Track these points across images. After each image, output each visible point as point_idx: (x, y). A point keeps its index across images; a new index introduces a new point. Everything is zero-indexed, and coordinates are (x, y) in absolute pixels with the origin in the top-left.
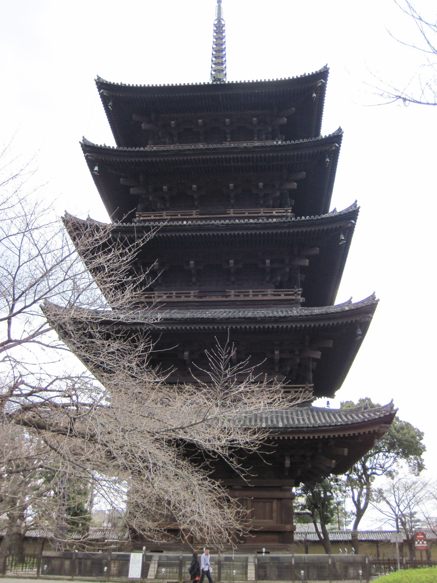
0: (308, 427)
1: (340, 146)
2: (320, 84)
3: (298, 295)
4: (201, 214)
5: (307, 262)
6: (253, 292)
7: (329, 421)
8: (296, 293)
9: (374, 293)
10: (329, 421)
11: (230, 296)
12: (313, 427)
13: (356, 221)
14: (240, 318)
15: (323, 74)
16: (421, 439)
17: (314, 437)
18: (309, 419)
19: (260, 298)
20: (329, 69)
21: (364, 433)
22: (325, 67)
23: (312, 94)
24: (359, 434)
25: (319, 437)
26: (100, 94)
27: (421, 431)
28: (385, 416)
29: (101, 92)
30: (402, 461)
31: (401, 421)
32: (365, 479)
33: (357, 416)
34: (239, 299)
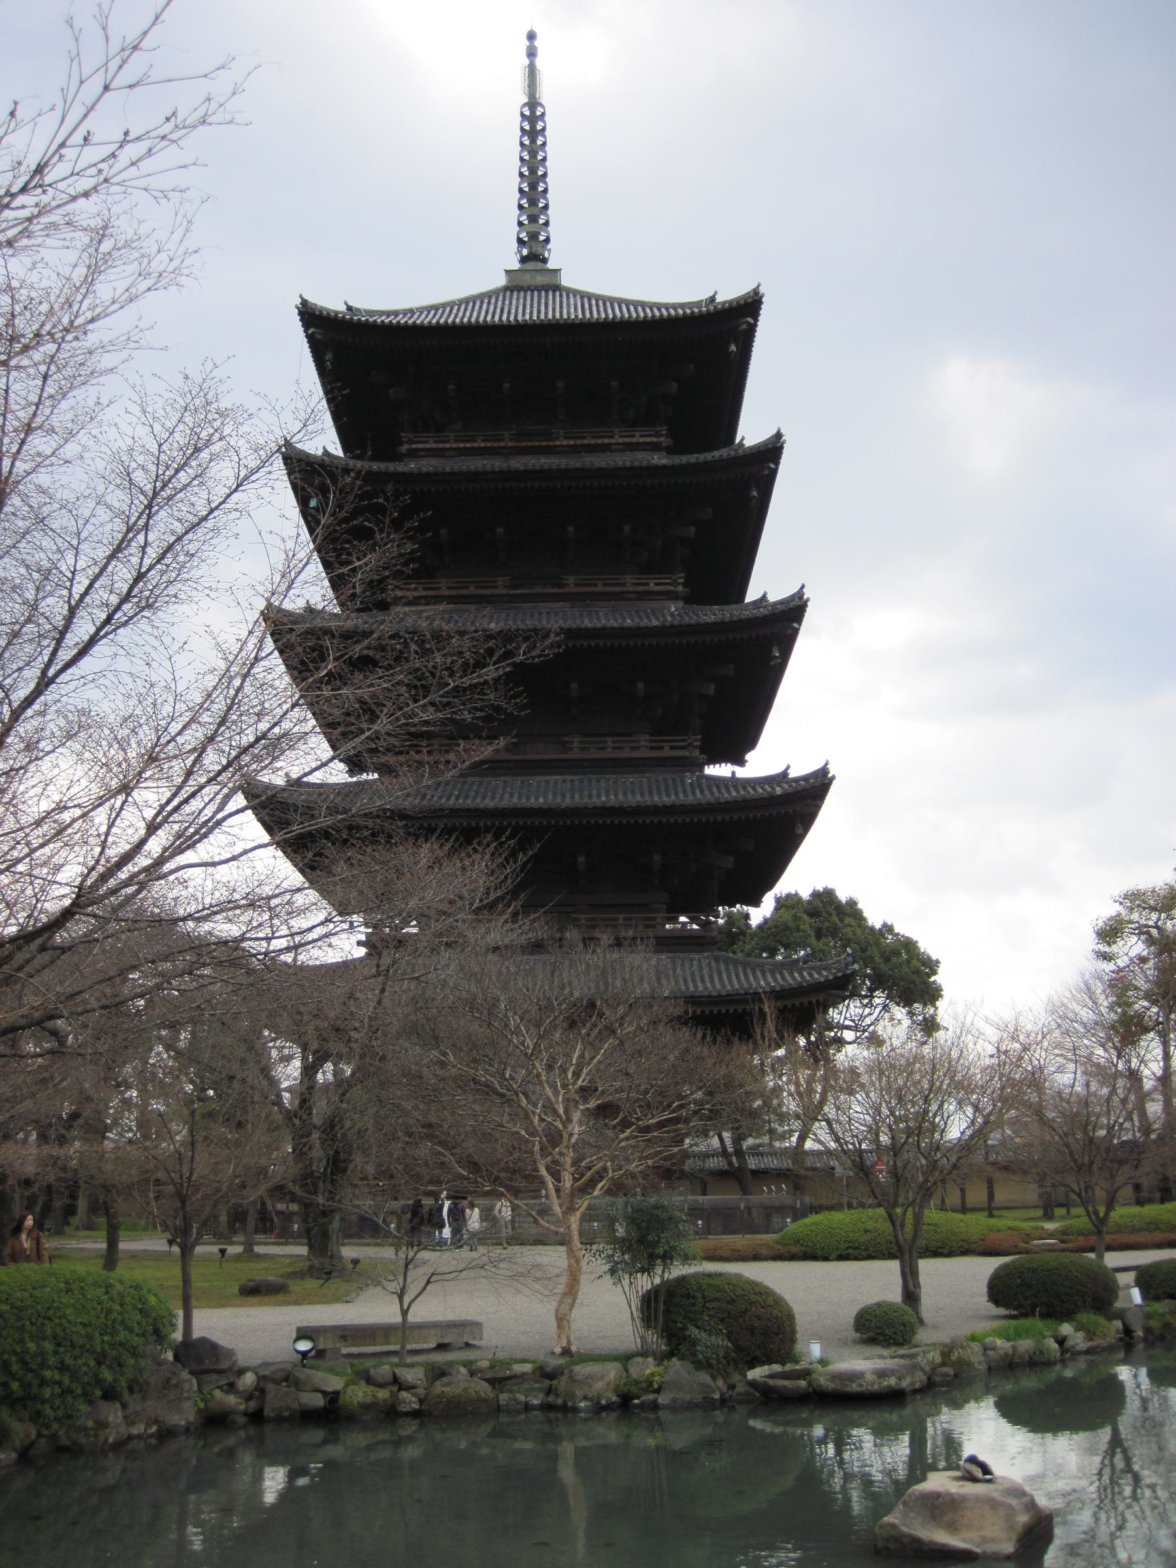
0: (710, 996)
1: (777, 468)
2: (744, 327)
3: (695, 747)
4: (515, 587)
5: (711, 689)
6: (613, 742)
7: (746, 985)
8: (690, 745)
9: (826, 764)
10: (746, 985)
11: (572, 749)
12: (719, 996)
13: (800, 624)
14: (595, 807)
15: (750, 306)
16: (934, 973)
17: (719, 1011)
18: (712, 981)
19: (626, 754)
20: (761, 297)
21: (801, 1004)
22: (756, 292)
23: (728, 345)
24: (794, 1005)
25: (727, 1011)
26: (307, 336)
27: (934, 958)
28: (836, 978)
29: (310, 331)
30: (899, 1012)
31: (898, 934)
32: (819, 1053)
33: (792, 975)
34: (587, 756)
